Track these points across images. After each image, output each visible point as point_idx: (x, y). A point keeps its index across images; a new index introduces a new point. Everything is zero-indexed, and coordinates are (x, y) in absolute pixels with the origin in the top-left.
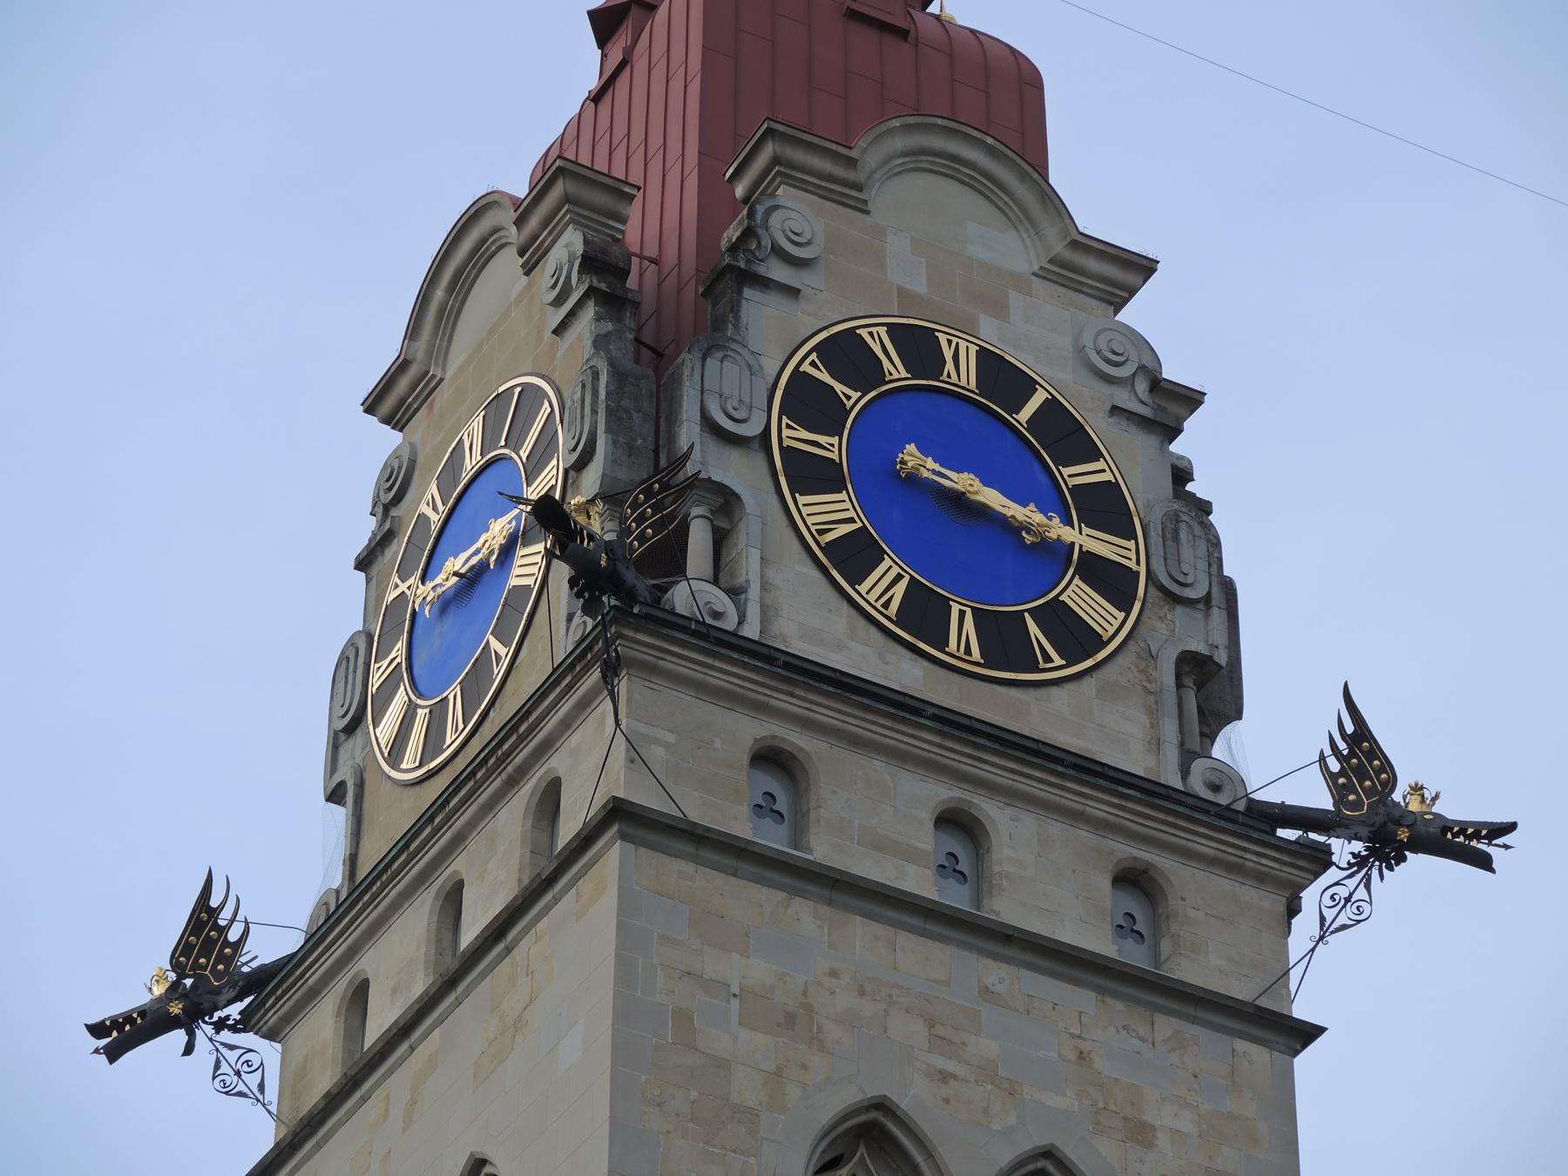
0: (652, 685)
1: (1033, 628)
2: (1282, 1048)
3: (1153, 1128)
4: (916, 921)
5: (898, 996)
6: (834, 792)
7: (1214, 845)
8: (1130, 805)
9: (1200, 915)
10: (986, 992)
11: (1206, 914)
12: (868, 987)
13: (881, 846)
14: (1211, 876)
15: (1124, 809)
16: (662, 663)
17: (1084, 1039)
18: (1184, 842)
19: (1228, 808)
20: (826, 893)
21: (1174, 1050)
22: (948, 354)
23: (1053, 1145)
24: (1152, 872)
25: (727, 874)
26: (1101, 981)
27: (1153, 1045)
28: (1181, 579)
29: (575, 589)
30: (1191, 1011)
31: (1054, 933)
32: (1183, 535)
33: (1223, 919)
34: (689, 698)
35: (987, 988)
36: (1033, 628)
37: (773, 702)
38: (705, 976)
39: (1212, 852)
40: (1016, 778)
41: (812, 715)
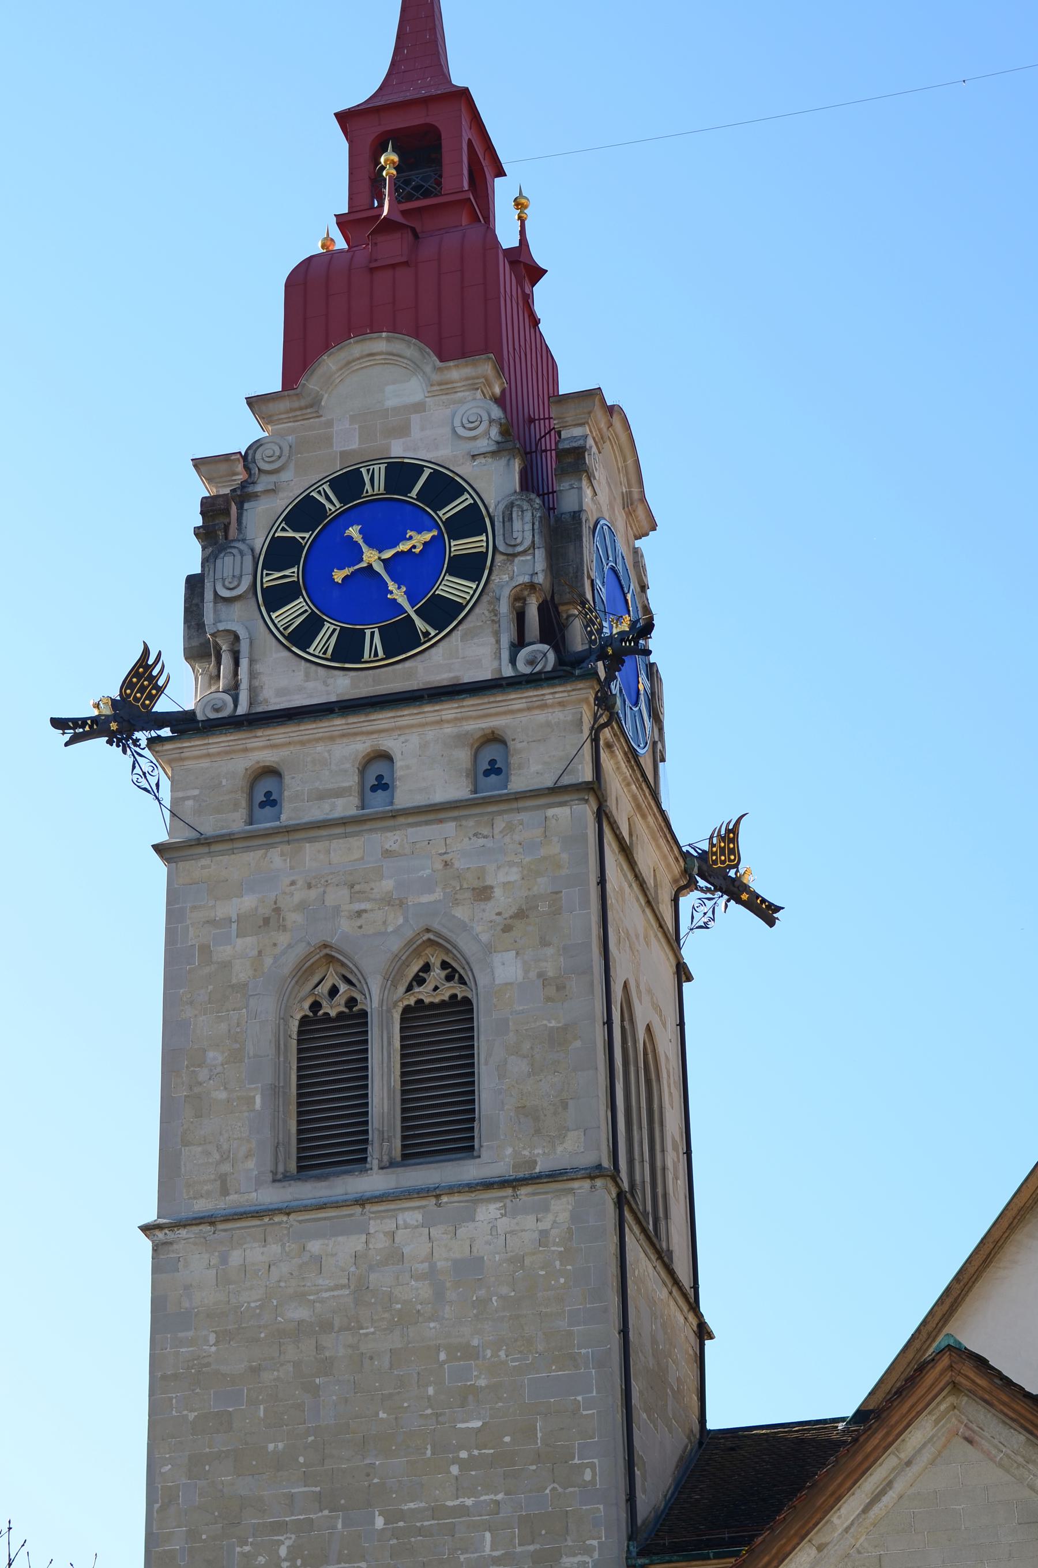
3: (492, 887)
4: (339, 830)
5: (332, 879)
6: (293, 778)
9: (525, 743)
12: (313, 882)
13: (321, 796)
15: (463, 706)
17: (448, 853)
18: (506, 707)
21: (506, 835)
26: (456, 813)
29: (115, 744)
33: (539, 740)
34: (207, 764)
38: (217, 919)
40: (395, 720)
41: (271, 742)
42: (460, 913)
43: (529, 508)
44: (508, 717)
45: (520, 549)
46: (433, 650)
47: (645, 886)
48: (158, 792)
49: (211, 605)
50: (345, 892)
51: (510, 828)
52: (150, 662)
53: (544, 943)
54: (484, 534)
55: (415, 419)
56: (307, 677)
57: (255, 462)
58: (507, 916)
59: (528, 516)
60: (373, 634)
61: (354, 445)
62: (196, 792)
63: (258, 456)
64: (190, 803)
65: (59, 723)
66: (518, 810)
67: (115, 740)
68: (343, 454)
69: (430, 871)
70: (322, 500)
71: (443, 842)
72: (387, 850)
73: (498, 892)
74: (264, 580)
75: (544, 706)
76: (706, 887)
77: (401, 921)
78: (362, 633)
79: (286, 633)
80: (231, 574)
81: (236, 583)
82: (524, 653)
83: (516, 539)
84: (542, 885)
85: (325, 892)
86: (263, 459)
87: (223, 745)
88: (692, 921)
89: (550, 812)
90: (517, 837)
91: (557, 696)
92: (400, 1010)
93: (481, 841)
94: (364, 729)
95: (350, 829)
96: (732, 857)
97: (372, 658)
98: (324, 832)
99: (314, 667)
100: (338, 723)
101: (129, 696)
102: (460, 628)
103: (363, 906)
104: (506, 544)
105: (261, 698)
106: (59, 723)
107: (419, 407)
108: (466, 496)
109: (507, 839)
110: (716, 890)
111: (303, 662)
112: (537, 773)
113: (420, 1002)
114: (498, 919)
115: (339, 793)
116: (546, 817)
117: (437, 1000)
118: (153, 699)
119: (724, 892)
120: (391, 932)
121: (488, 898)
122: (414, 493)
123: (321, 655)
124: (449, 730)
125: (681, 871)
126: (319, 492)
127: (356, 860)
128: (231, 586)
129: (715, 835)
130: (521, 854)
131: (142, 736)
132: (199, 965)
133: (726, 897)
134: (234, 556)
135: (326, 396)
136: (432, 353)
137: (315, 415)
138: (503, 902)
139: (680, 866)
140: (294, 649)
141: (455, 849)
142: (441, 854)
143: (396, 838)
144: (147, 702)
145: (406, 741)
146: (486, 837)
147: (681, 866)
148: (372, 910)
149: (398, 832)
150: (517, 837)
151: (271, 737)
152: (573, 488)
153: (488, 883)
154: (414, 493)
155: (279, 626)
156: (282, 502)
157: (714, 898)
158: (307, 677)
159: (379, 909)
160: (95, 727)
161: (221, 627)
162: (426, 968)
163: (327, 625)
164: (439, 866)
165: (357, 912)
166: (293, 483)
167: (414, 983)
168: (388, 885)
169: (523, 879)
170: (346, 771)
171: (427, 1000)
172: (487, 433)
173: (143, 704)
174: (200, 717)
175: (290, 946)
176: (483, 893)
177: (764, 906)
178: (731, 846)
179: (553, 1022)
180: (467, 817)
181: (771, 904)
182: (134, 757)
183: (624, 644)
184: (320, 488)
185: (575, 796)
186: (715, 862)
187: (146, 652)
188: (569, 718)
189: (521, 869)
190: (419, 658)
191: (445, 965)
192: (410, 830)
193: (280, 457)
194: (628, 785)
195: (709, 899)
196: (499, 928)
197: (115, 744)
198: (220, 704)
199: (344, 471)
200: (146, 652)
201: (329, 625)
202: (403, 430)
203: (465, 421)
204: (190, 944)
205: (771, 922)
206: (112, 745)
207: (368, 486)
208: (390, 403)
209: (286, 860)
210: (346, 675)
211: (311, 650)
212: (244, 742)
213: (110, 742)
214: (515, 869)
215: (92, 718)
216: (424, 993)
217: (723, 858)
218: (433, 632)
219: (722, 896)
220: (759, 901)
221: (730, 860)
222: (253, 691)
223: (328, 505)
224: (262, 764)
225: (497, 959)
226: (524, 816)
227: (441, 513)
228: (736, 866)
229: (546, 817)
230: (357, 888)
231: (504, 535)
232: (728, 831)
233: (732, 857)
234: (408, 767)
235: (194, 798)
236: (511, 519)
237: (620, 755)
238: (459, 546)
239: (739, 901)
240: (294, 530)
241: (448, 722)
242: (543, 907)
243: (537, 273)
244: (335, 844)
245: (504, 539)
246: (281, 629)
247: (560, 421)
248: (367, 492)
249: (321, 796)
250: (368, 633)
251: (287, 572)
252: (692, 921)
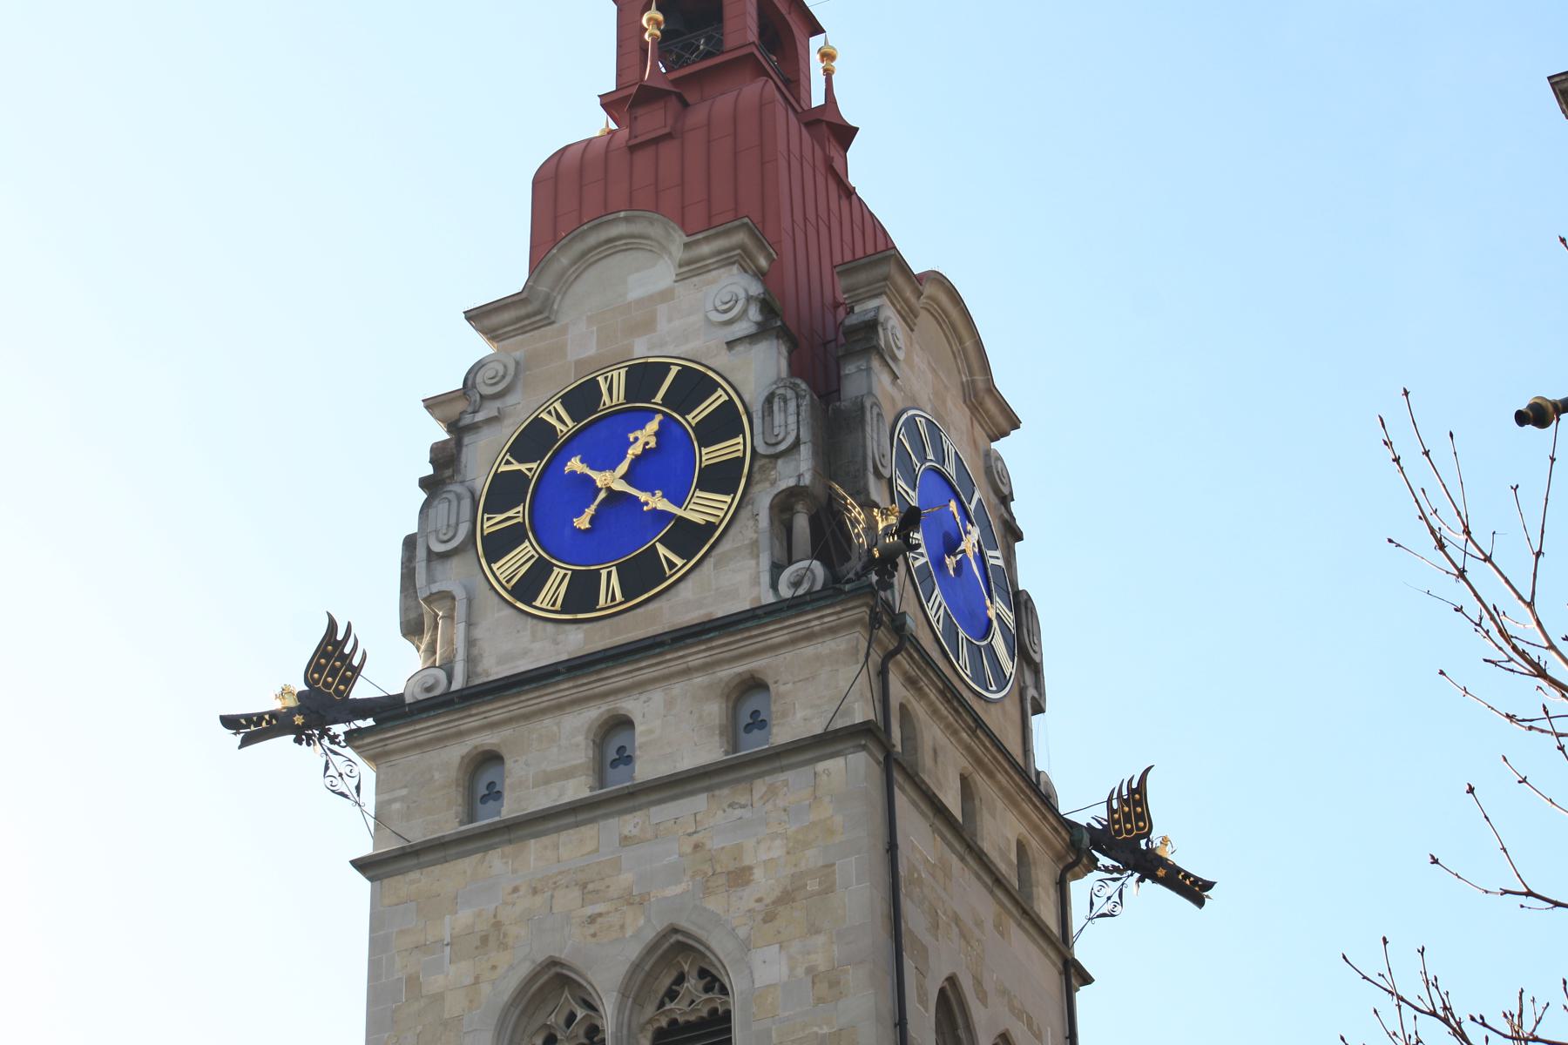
0: (393, 763)
2: (852, 750)
3: (750, 868)
4: (570, 820)
7: (785, 631)
8: (714, 644)
9: (789, 686)
10: (626, 841)
11: (794, 683)
13: (547, 779)
14: (797, 651)
16: (387, 748)
20: (506, 837)
21: (768, 801)
23: (672, 924)
24: (756, 675)
25: (441, 863)
26: (706, 783)
27: (752, 805)
29: (304, 743)
30: (777, 764)
31: (675, 767)
33: (807, 679)
37: (462, 727)
38: (428, 943)
39: (787, 637)
41: (489, 720)
42: (714, 904)
43: (794, 395)
44: (769, 655)
45: (782, 447)
46: (682, 586)
47: (984, 858)
48: (358, 795)
49: (424, 564)
50: (576, 893)
51: (772, 791)
52: (340, 637)
53: (815, 930)
54: (741, 436)
55: (662, 309)
56: (534, 638)
57: (475, 387)
58: (768, 901)
59: (792, 406)
60: (609, 574)
61: (591, 350)
62: (404, 792)
63: (479, 379)
64: (396, 806)
65: (230, 722)
66: (782, 769)
67: (304, 737)
68: (579, 364)
69: (677, 856)
70: (553, 421)
71: (692, 818)
72: (626, 837)
73: (758, 874)
74: (485, 527)
75: (810, 637)
76: (1113, 866)
77: (641, 922)
78: (597, 574)
79: (509, 586)
80: (445, 523)
81: (450, 534)
82: (787, 575)
83: (777, 436)
84: (812, 858)
85: (552, 897)
86: (484, 382)
87: (432, 730)
88: (1091, 908)
89: (821, 766)
90: (781, 803)
91: (826, 620)
92: (649, 1034)
93: (738, 812)
94: (596, 690)
95: (581, 817)
96: (1141, 824)
97: (609, 604)
98: (551, 825)
99: (541, 624)
100: (565, 689)
101: (317, 682)
102: (714, 553)
103: (600, 908)
104: (766, 443)
105: (479, 669)
106: (230, 722)
107: (665, 296)
108: (720, 392)
109: (769, 806)
110: (1127, 867)
111: (529, 619)
112: (805, 720)
113: (673, 1022)
114: (758, 906)
115: (567, 774)
116: (815, 774)
117: (692, 1018)
118: (349, 682)
119: (1135, 869)
120: (631, 936)
121: (748, 882)
122: (658, 398)
123: (549, 607)
124: (700, 680)
125: (1067, 846)
126: (549, 412)
127: (589, 853)
128: (446, 538)
129: (1115, 796)
130: (785, 822)
131: (339, 729)
132: (406, 1001)
133: (1137, 875)
134: (450, 501)
135: (559, 298)
136: (676, 227)
137: (545, 322)
138: (764, 884)
139: (1063, 839)
140: (519, 605)
141: (707, 826)
142: (690, 835)
143: (636, 820)
144: (342, 687)
145: (649, 699)
146: (743, 807)
147: (1063, 839)
148: (608, 913)
149: (639, 813)
150: (781, 803)
151: (487, 715)
152: (862, 370)
153: (747, 862)
154: (658, 398)
155: (501, 579)
156: (509, 432)
157: (1121, 878)
158: (534, 638)
159: (616, 910)
160: (274, 722)
161: (435, 588)
162: (681, 979)
163: (556, 570)
164: (688, 849)
165: (589, 917)
166: (519, 407)
167: (667, 1000)
168: (626, 878)
169: (788, 853)
170: (578, 745)
171: (681, 1020)
172: (745, 312)
173: (337, 691)
174: (408, 700)
175: (512, 967)
176: (740, 877)
177: (1188, 882)
178: (1139, 809)
179: (825, 1027)
180: (720, 786)
181: (1197, 879)
182: (327, 755)
183: (887, 541)
184: (551, 408)
185: (850, 744)
186: (1119, 832)
187: (332, 626)
188: (843, 647)
189: (785, 841)
190: (664, 597)
191: (703, 973)
192: (653, 810)
193: (503, 377)
194: (955, 733)
195: (1114, 880)
196: (759, 917)
197: (304, 743)
198: (430, 682)
199: (579, 382)
200: (332, 626)
201: (559, 570)
202: (648, 325)
203: (718, 303)
204: (396, 977)
205: (1199, 902)
206: (301, 744)
207: (605, 397)
208: (635, 293)
209: (507, 863)
210: (579, 628)
211: (537, 603)
212: (456, 723)
213: (298, 741)
214: (778, 842)
215: (273, 714)
216: (680, 1010)
217: (1129, 826)
218: (679, 562)
219: (1132, 875)
220: (1180, 877)
221: (1138, 828)
222: (471, 660)
223: (559, 426)
224: (480, 749)
225: (757, 957)
226: (789, 775)
227: (689, 417)
228: (1147, 835)
229: (815, 774)
230: (591, 887)
231: (763, 433)
232: (1131, 791)
233: (1141, 824)
234: (651, 731)
235: (402, 799)
236: (771, 412)
237: (933, 695)
238: (709, 455)
239: (1156, 879)
240: (520, 461)
241: (698, 669)
242: (813, 886)
243: (846, 134)
244: (564, 836)
245: (764, 438)
246: (504, 582)
247: (851, 294)
248: (604, 404)
249: (547, 779)
250: (604, 573)
251: (511, 513)
252: (1091, 908)
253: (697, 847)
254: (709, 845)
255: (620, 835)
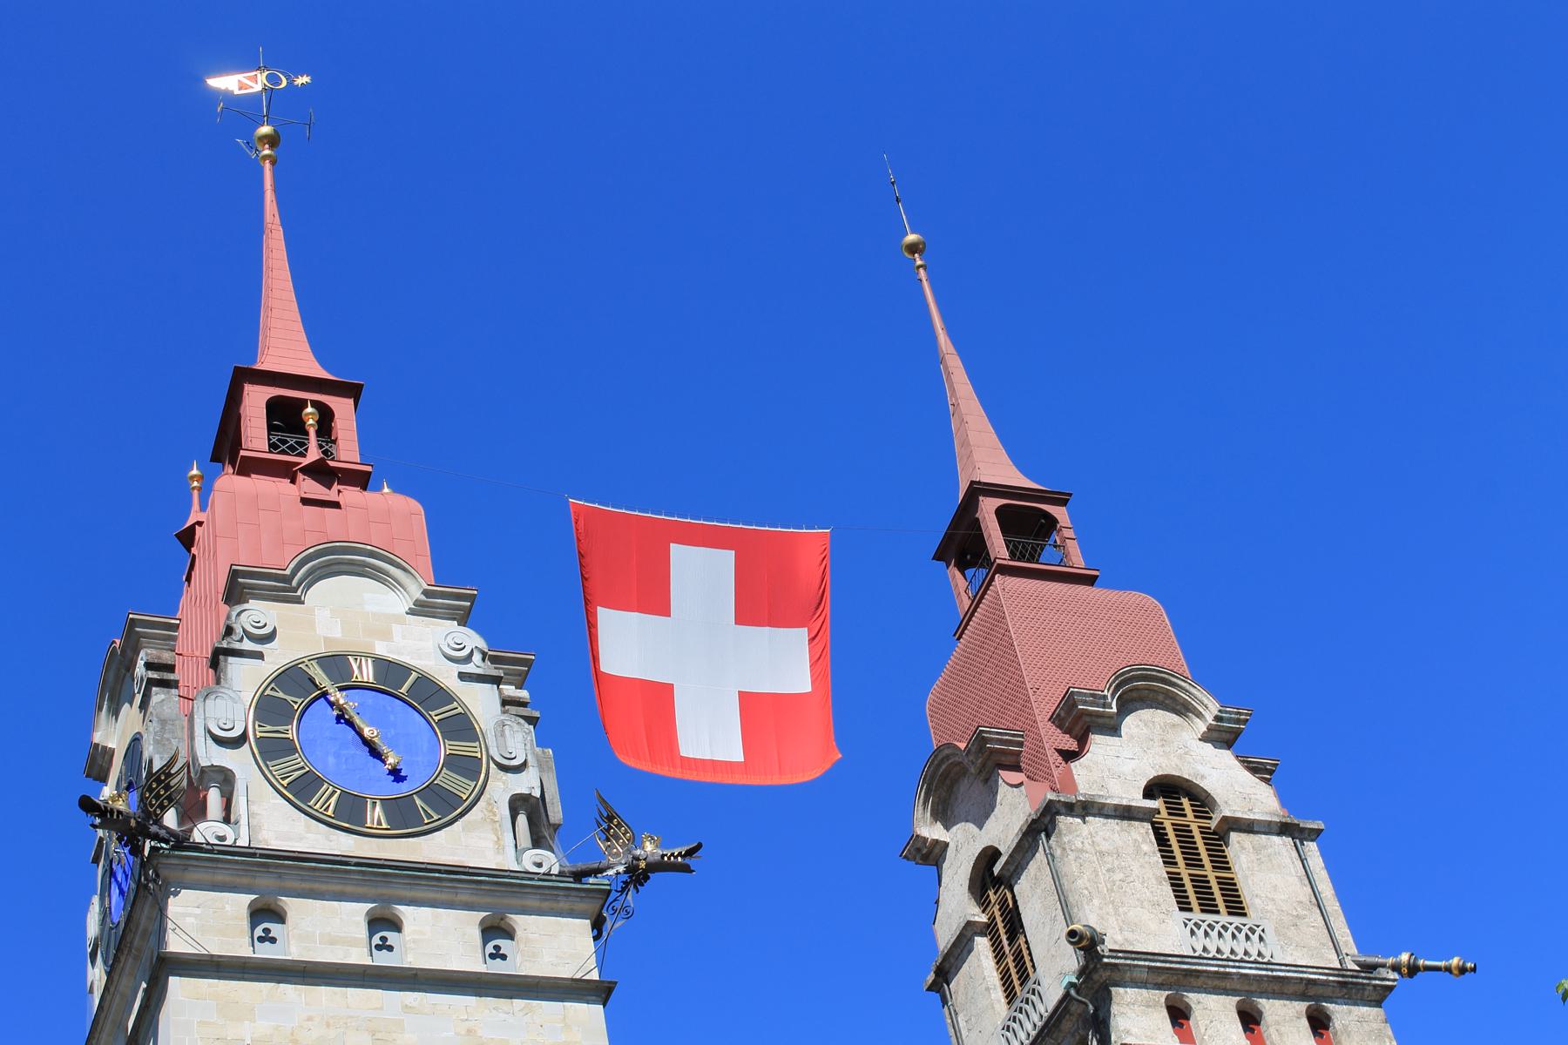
1: (418, 802)
13: (333, 942)
19: (548, 874)
22: (355, 667)
28: (509, 756)
32: (507, 732)
35: (406, 1006)
36: (418, 802)
142: (462, 1020)
173: (155, 810)
249: (333, 942)
253: (469, 1031)
254: (480, 1033)
255: (402, 1002)
